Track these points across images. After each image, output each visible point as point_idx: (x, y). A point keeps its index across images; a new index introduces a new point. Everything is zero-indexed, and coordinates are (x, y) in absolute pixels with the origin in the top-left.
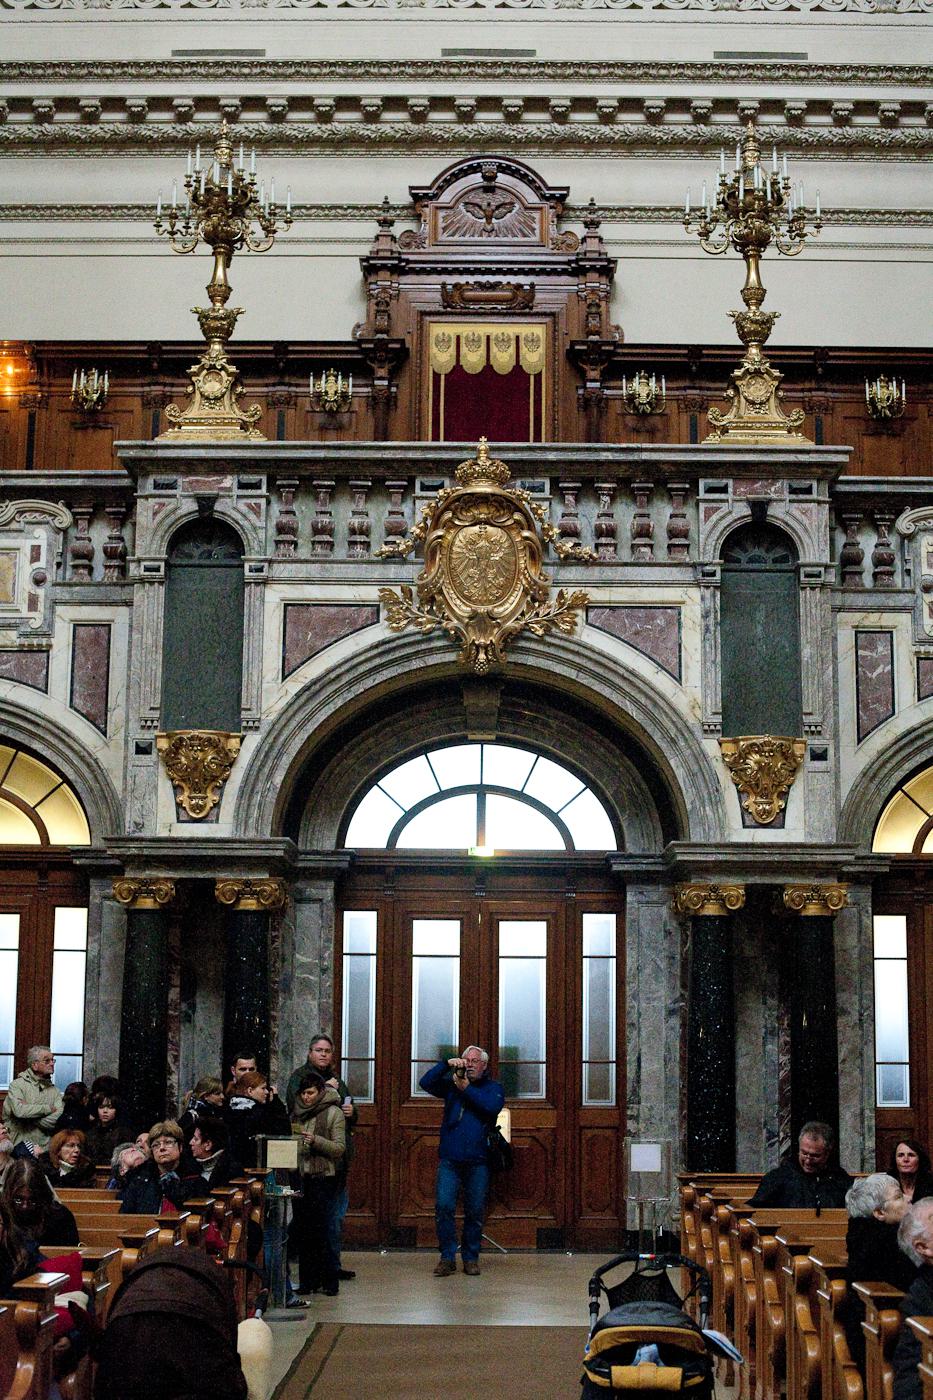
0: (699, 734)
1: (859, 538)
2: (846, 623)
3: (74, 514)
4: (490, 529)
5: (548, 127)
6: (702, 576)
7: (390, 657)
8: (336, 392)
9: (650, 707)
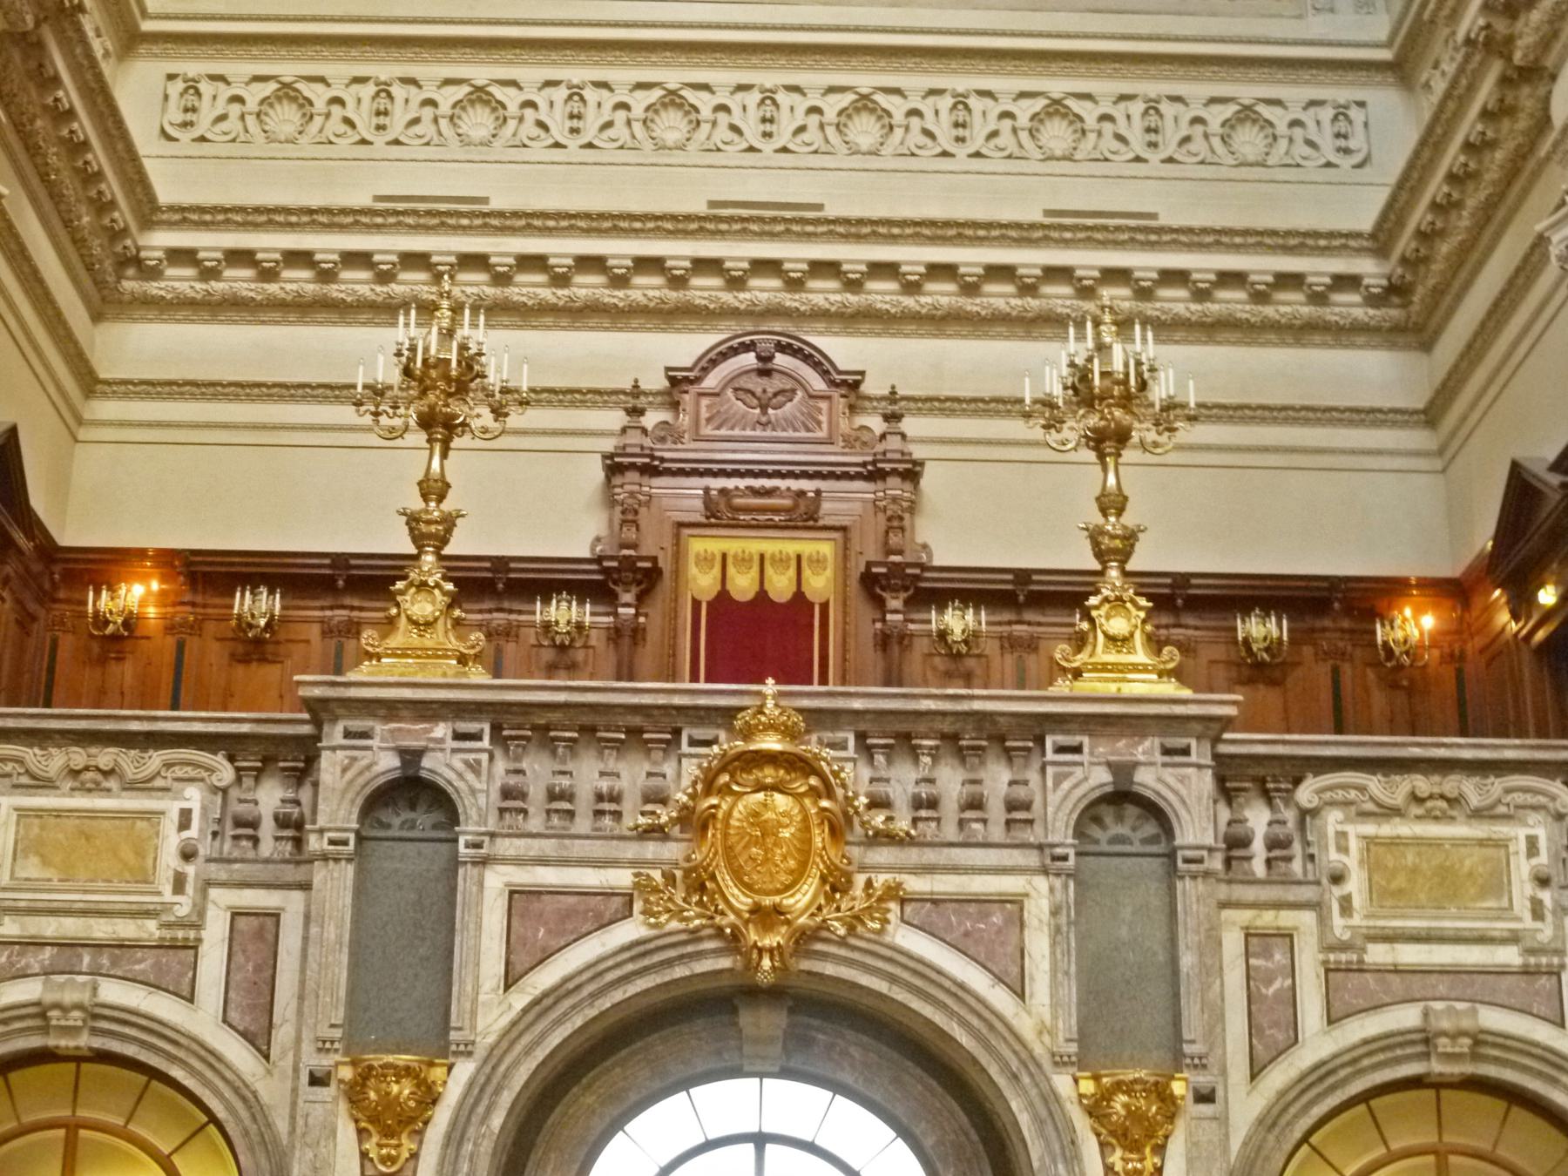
1: (1248, 813)
2: (1234, 923)
3: (238, 769)
4: (778, 797)
5: (838, 297)
6: (1050, 862)
7: (646, 962)
8: (569, 622)
9: (985, 1031)
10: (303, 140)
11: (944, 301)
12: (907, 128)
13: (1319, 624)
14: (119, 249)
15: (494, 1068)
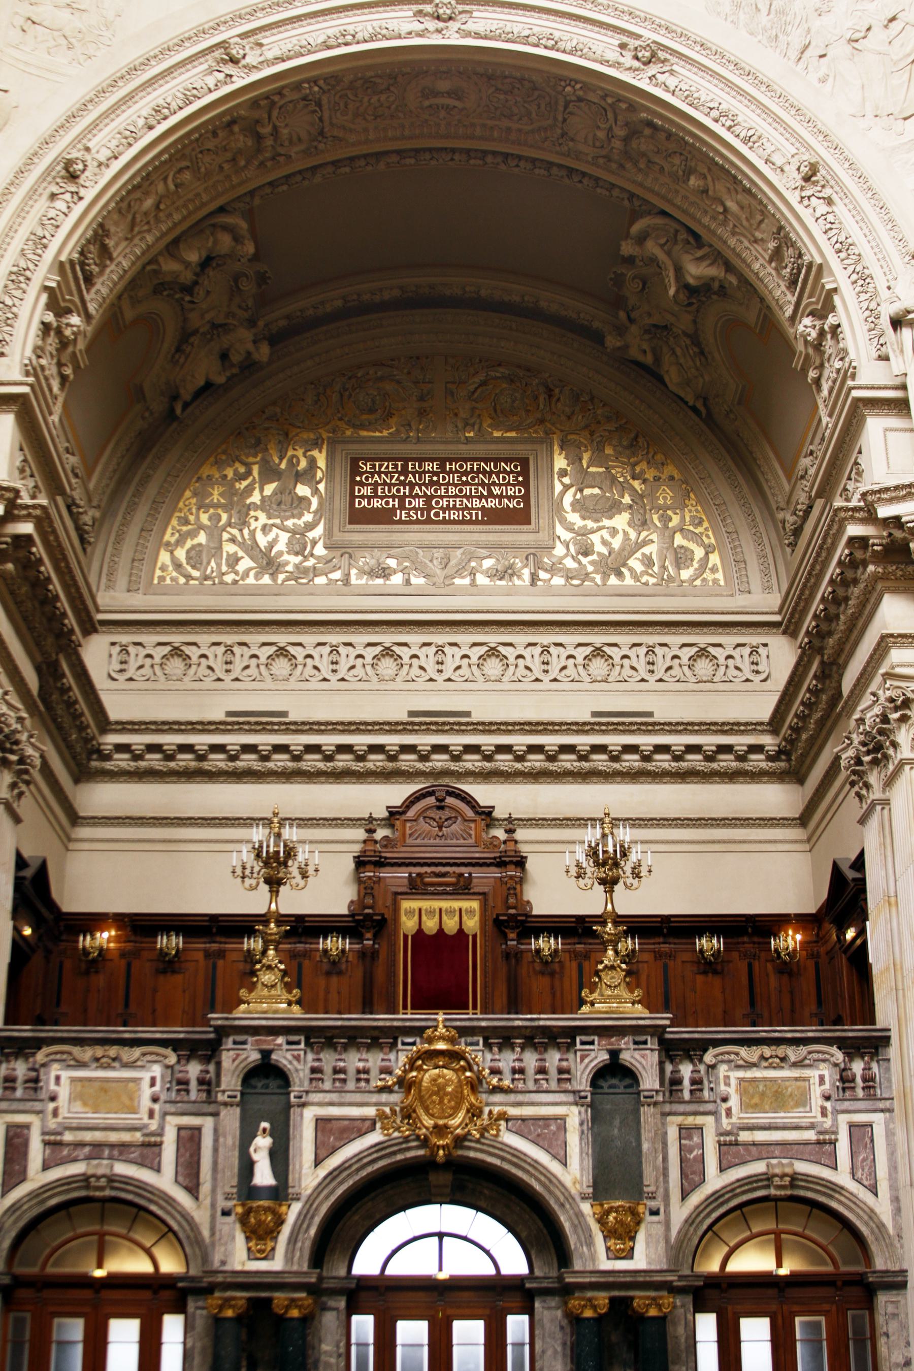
0: (578, 1199)
3: (178, 1056)
4: (445, 1071)
5: (480, 764)
6: (578, 1099)
7: (383, 1153)
9: (547, 1182)
10: (186, 679)
11: (537, 764)
12: (516, 666)
13: (740, 940)
14: (89, 746)
15: (311, 1205)
